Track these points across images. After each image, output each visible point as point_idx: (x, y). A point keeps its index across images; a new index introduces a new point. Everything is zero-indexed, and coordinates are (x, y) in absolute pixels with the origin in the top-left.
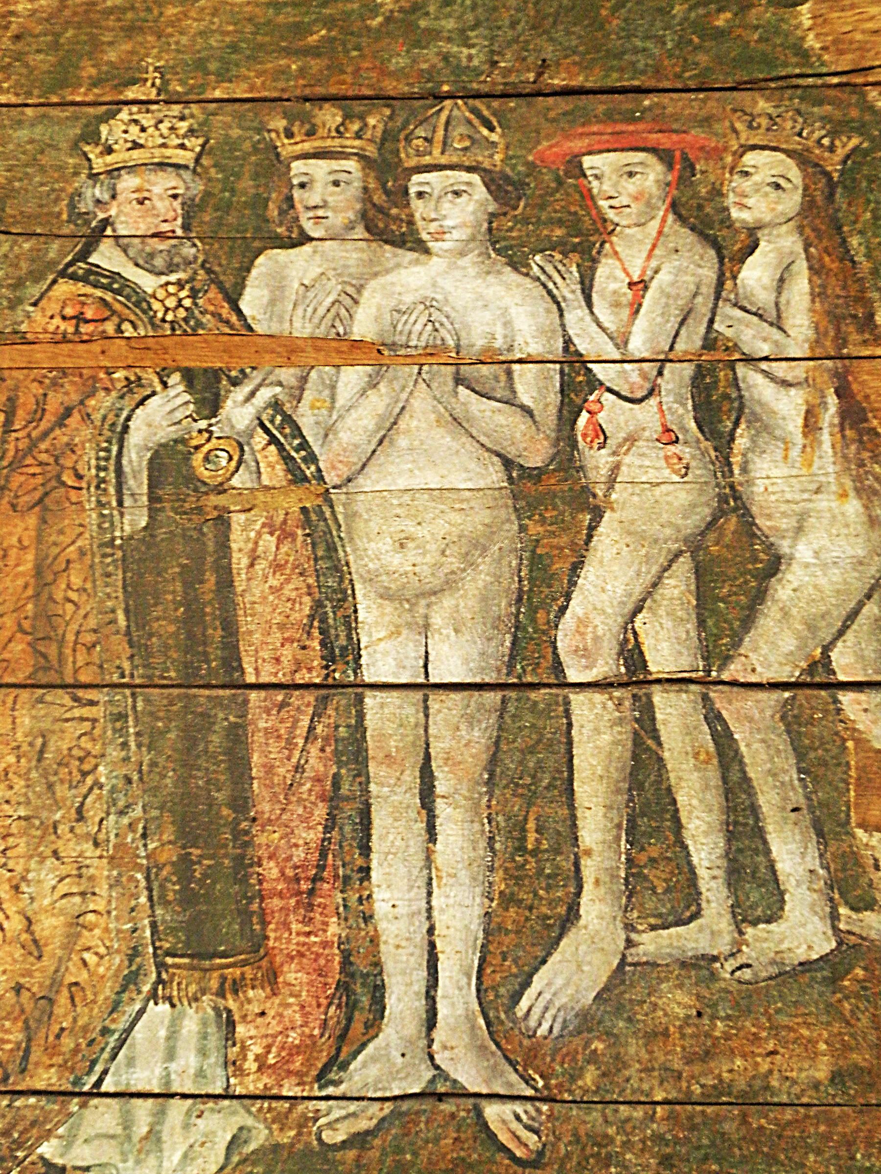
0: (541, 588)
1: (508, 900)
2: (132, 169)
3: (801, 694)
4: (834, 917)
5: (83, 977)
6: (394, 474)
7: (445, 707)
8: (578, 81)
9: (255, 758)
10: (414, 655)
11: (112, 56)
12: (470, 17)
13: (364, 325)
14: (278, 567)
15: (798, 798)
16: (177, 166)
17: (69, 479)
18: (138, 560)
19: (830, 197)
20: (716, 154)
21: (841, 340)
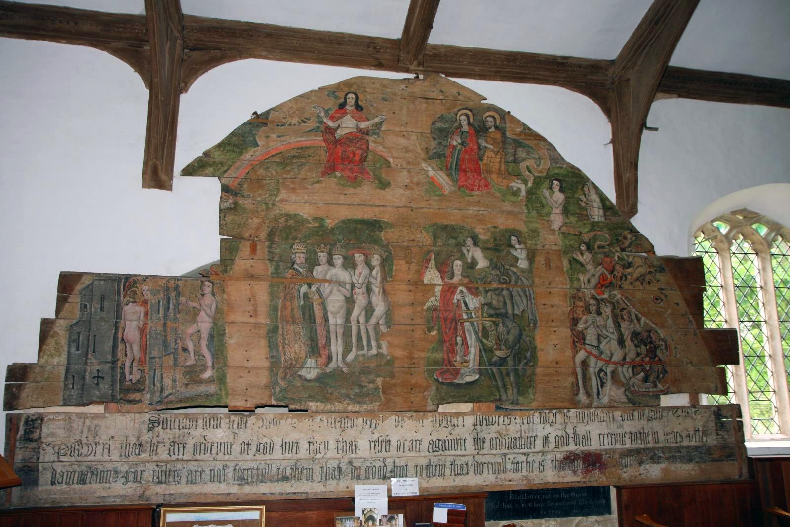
0: (349, 312)
2: (299, 253)
10: (335, 320)
13: (328, 277)
18: (303, 308)
20: (371, 254)
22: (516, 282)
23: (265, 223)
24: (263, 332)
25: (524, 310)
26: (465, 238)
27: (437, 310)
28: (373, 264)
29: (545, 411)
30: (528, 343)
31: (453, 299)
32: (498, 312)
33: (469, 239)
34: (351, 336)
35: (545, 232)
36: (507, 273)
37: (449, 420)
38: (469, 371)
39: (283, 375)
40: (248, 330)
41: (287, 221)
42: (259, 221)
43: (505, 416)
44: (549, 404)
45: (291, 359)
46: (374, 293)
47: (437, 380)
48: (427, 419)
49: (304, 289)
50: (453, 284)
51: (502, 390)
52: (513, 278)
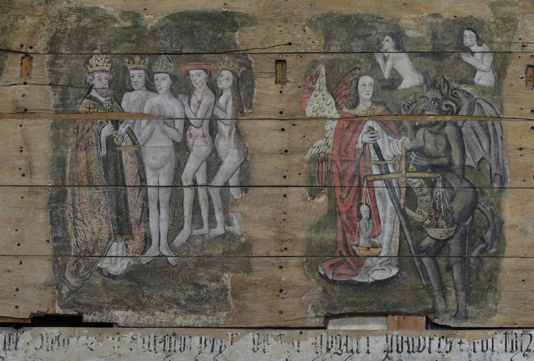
0: (179, 167)
1: (172, 225)
2: (98, 71)
3: (223, 188)
4: (225, 227)
5: (102, 238)
6: (152, 144)
7: (162, 190)
8: (189, 51)
9: (129, 200)
10: (156, 180)
11: (90, 41)
12: (166, 33)
13: (146, 111)
14: (131, 163)
15: (221, 207)
16: (106, 71)
17: (91, 144)
18: (105, 161)
19: (238, 82)
20: (216, 71)
21: (237, 115)
22: (471, 110)
23: (44, 24)
24: (42, 200)
25: (482, 159)
26: (381, 37)
27: (327, 161)
28: (220, 86)
29: (515, 331)
30: (489, 215)
31: (357, 143)
32: (435, 162)
33: (387, 37)
34: (183, 206)
35: (527, 21)
36: (455, 95)
37: (344, 341)
38: (379, 261)
39: (73, 268)
40: (19, 198)
41: (79, 19)
42: (35, 21)
43: (443, 337)
44: (524, 319)
45: (86, 243)
46: (222, 135)
47: (324, 277)
48: (306, 339)
49: (107, 130)
50: (357, 116)
51: (436, 293)
52: (465, 104)
